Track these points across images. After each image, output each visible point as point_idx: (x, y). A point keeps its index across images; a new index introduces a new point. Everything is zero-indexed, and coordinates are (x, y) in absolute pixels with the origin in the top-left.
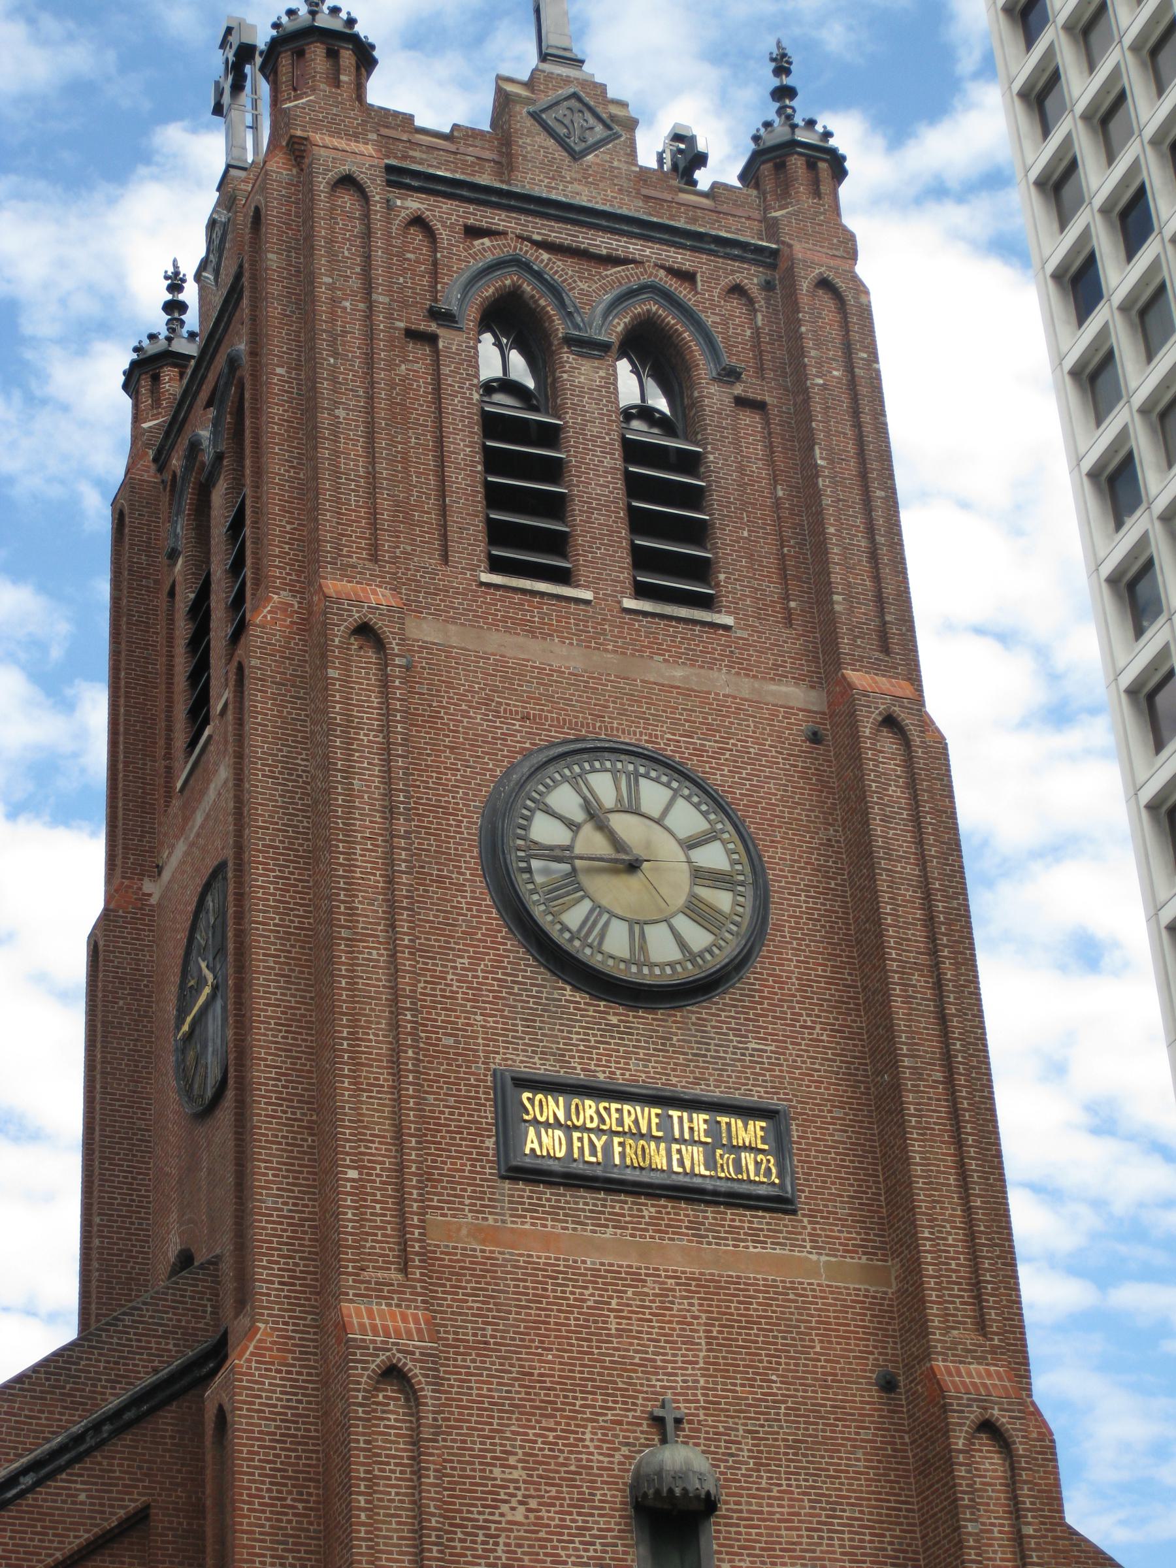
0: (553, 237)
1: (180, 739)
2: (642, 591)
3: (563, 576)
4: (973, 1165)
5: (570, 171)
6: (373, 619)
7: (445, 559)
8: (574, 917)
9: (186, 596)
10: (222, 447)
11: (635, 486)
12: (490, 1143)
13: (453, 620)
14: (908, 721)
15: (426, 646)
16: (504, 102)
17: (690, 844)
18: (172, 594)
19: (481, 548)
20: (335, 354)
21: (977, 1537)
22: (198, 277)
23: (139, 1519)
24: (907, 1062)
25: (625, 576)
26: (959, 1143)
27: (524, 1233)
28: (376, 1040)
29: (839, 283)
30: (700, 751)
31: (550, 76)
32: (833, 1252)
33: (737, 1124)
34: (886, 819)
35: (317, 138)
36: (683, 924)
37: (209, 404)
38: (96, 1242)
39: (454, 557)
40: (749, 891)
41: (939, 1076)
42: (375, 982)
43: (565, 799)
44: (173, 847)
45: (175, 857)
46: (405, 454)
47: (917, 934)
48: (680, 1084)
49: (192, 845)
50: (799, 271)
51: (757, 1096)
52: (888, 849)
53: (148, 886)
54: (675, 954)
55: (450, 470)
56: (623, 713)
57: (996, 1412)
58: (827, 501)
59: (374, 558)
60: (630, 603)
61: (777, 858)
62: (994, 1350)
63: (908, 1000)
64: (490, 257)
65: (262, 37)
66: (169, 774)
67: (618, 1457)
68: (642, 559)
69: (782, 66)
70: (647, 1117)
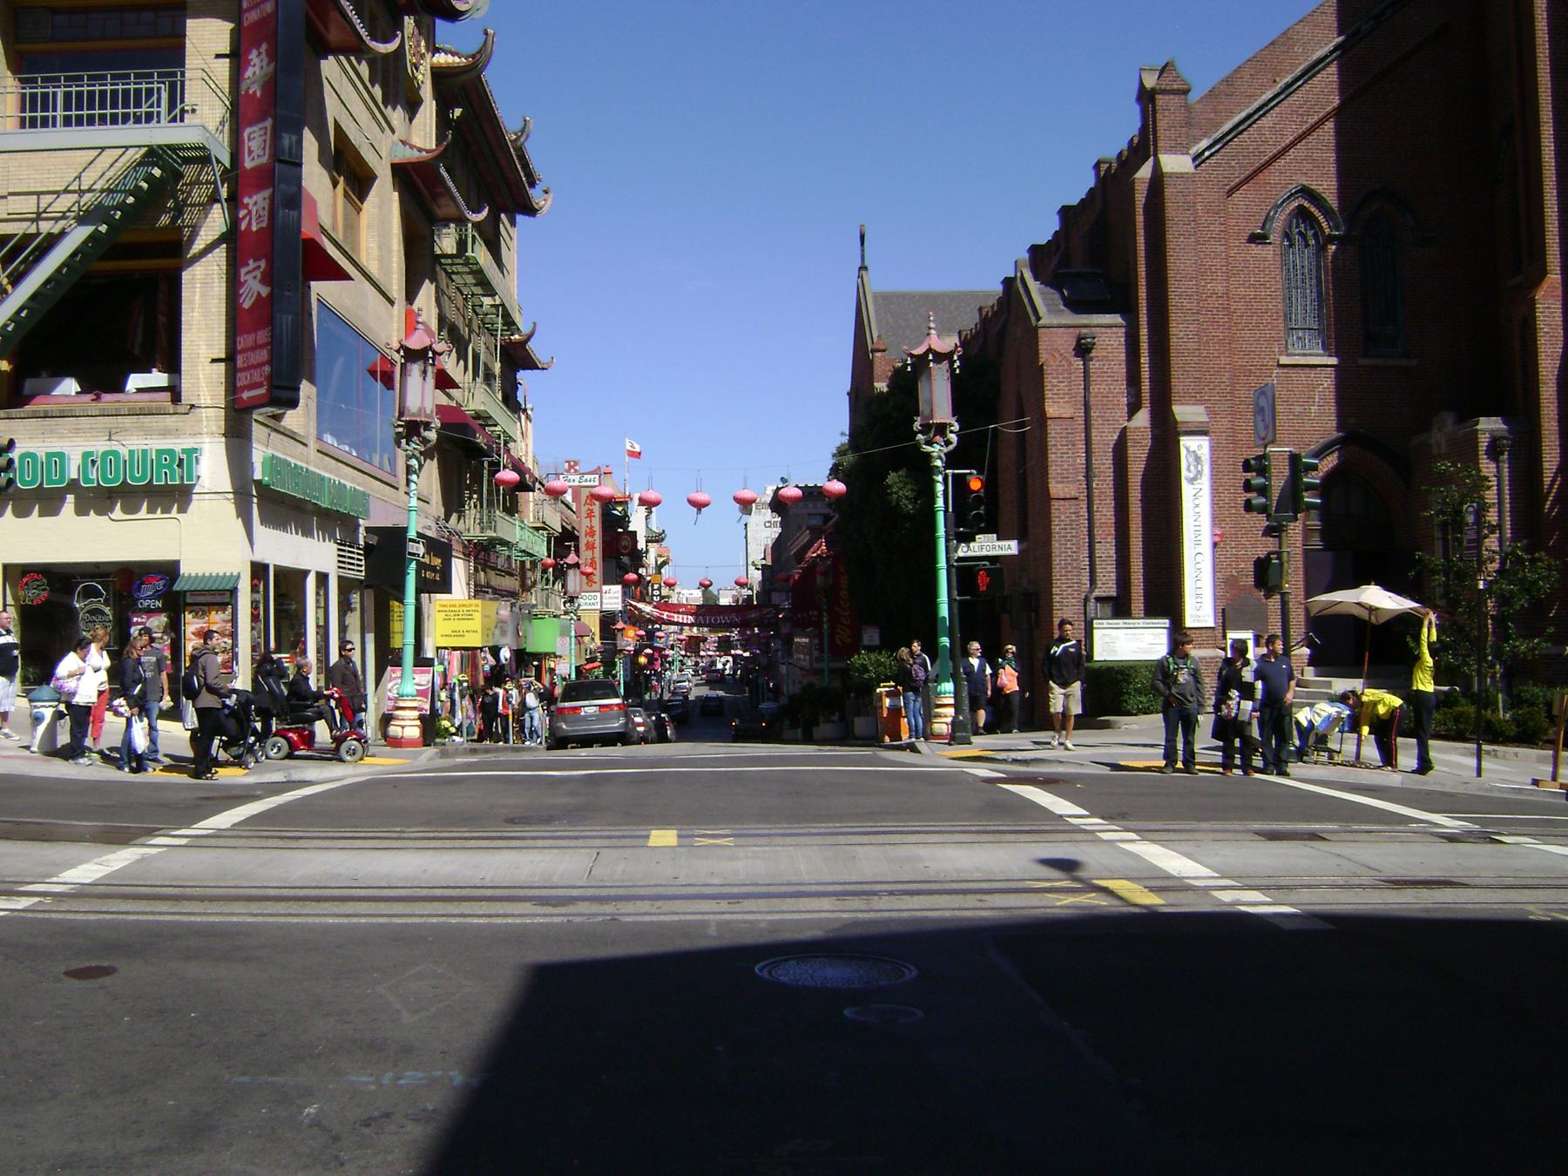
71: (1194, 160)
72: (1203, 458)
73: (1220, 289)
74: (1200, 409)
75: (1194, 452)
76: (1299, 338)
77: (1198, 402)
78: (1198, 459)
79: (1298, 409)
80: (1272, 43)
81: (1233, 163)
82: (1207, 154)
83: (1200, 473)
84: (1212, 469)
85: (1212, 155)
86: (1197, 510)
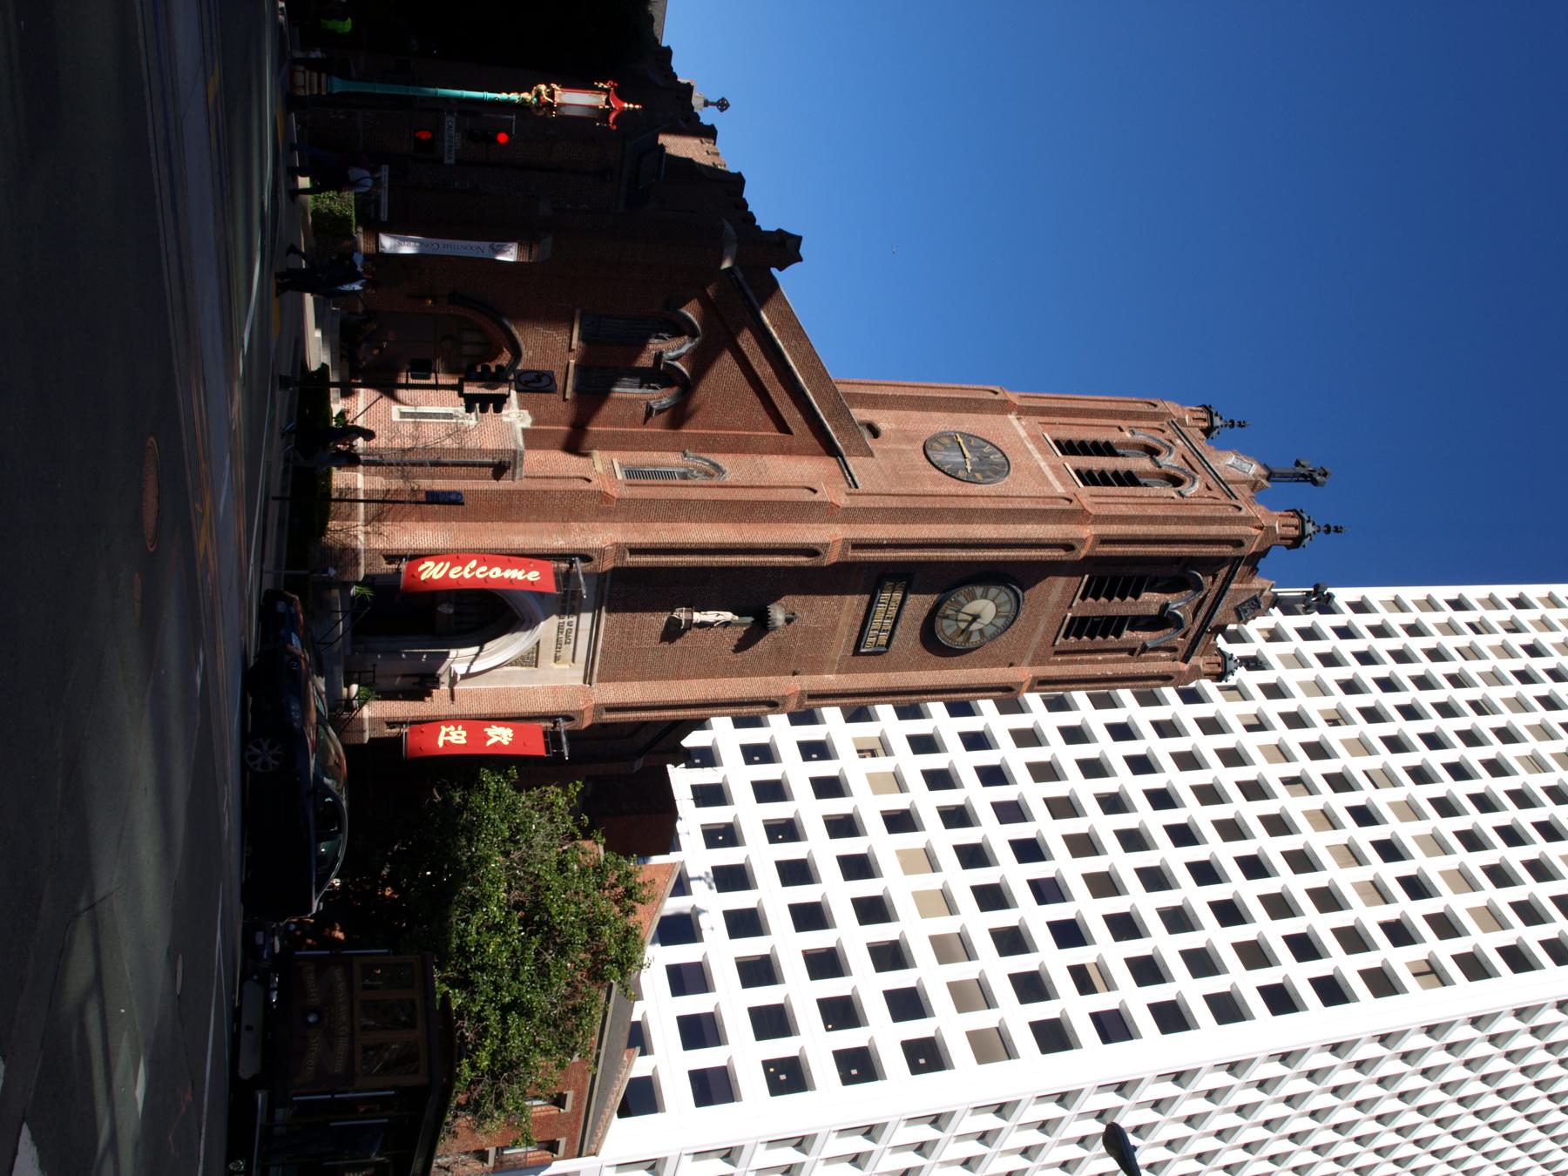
0: (1208, 599)
2: (1073, 619)
3: (1083, 597)
5: (1232, 606)
8: (962, 599)
9: (1113, 437)
10: (1163, 468)
23: (788, 431)
44: (1024, 428)
48: (902, 622)
49: (1021, 440)
51: (894, 643)
60: (1069, 615)
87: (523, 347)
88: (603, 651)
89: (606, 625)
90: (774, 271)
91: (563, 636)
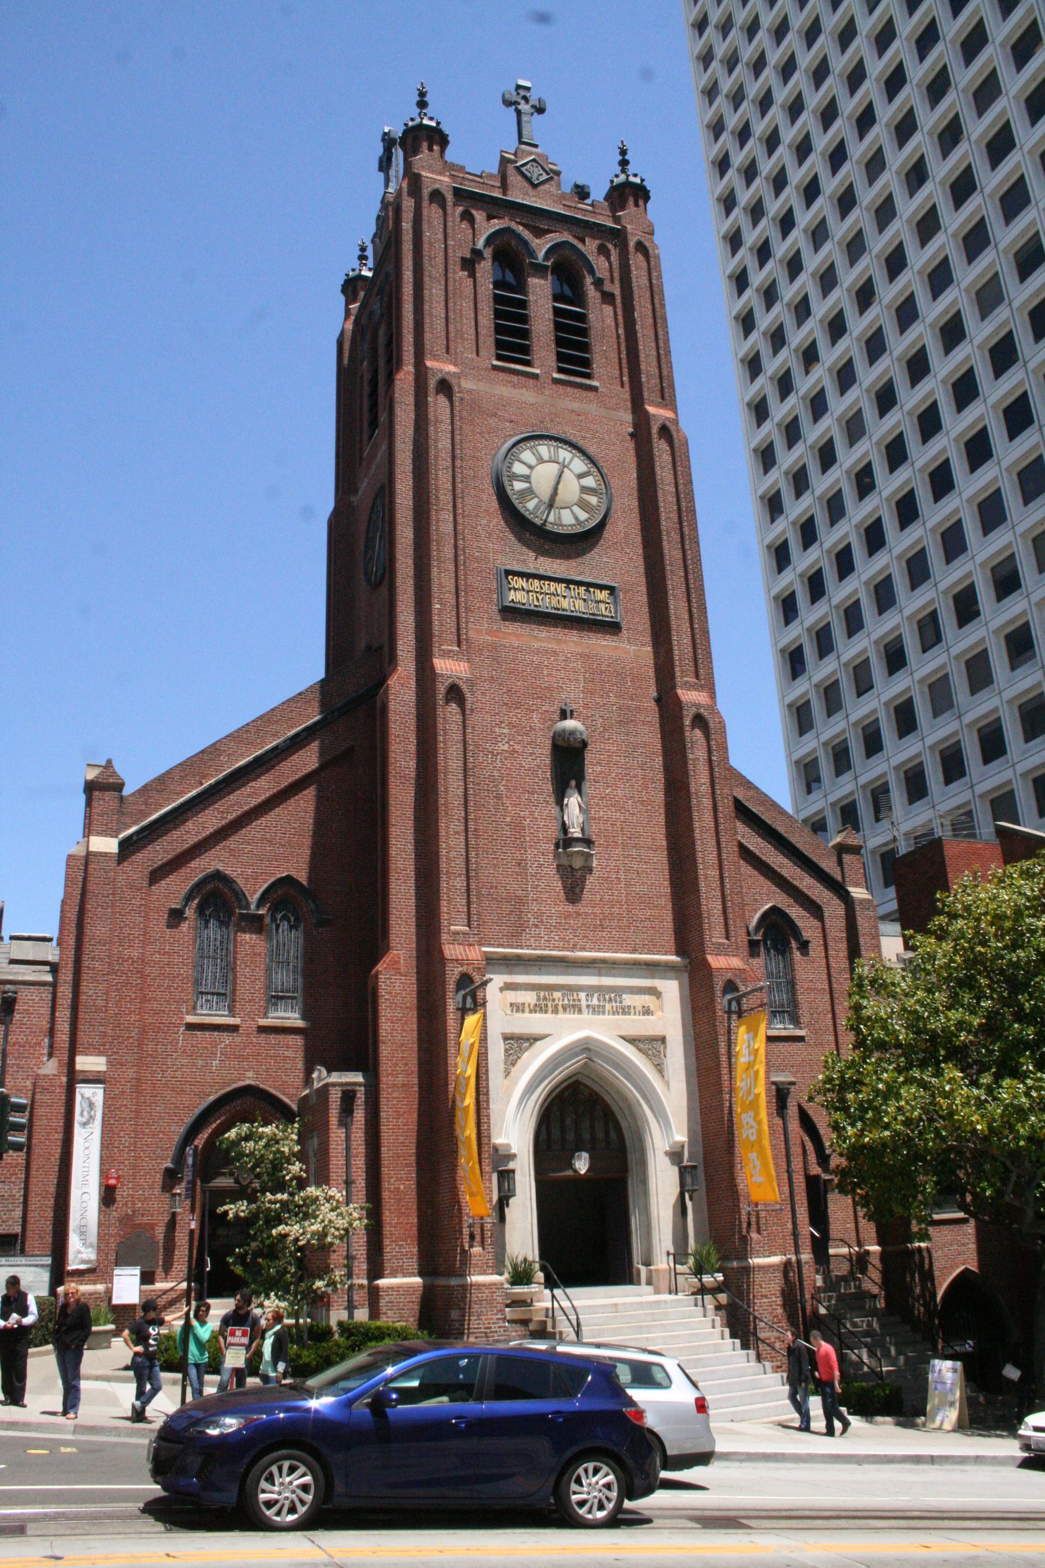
1: (365, 437)
2: (560, 370)
4: (695, 610)
6: (447, 377)
7: (478, 355)
8: (531, 505)
9: (367, 377)
11: (558, 327)
12: (495, 596)
13: (481, 380)
14: (672, 428)
15: (470, 391)
16: (504, 162)
17: (580, 476)
18: (362, 377)
19: (493, 350)
20: (431, 265)
21: (694, 760)
22: (373, 241)
24: (668, 568)
25: (554, 364)
26: (689, 601)
27: (509, 634)
28: (448, 551)
29: (646, 244)
30: (584, 438)
31: (523, 151)
32: (636, 645)
33: (598, 592)
34: (662, 468)
35: (424, 173)
36: (576, 509)
37: (377, 295)
38: (332, 643)
39: (481, 354)
40: (604, 496)
41: (682, 574)
42: (447, 528)
43: (527, 456)
45: (363, 486)
46: (461, 310)
47: (674, 516)
50: (629, 237)
52: (662, 479)
53: (353, 499)
54: (573, 521)
55: (480, 318)
56: (552, 421)
57: (702, 710)
58: (639, 335)
59: (448, 352)
60: (556, 375)
61: (615, 482)
62: (702, 686)
63: (669, 542)
64: (497, 228)
65: (398, 132)
66: (361, 450)
67: (547, 725)
68: (561, 357)
69: (623, 152)
70: (561, 588)
71: (121, 844)
72: (96, 1104)
73: (135, 954)
74: (102, 1060)
75: (88, 1099)
76: (207, 1001)
77: (100, 1053)
78: (91, 1105)
79: (200, 1063)
80: (202, 752)
81: (161, 851)
82: (135, 838)
83: (92, 1118)
84: (104, 1114)
85: (139, 839)
86: (87, 1152)
87: (241, 1084)
88: (634, 951)
89: (591, 950)
90: (127, 791)
91: (608, 1007)
